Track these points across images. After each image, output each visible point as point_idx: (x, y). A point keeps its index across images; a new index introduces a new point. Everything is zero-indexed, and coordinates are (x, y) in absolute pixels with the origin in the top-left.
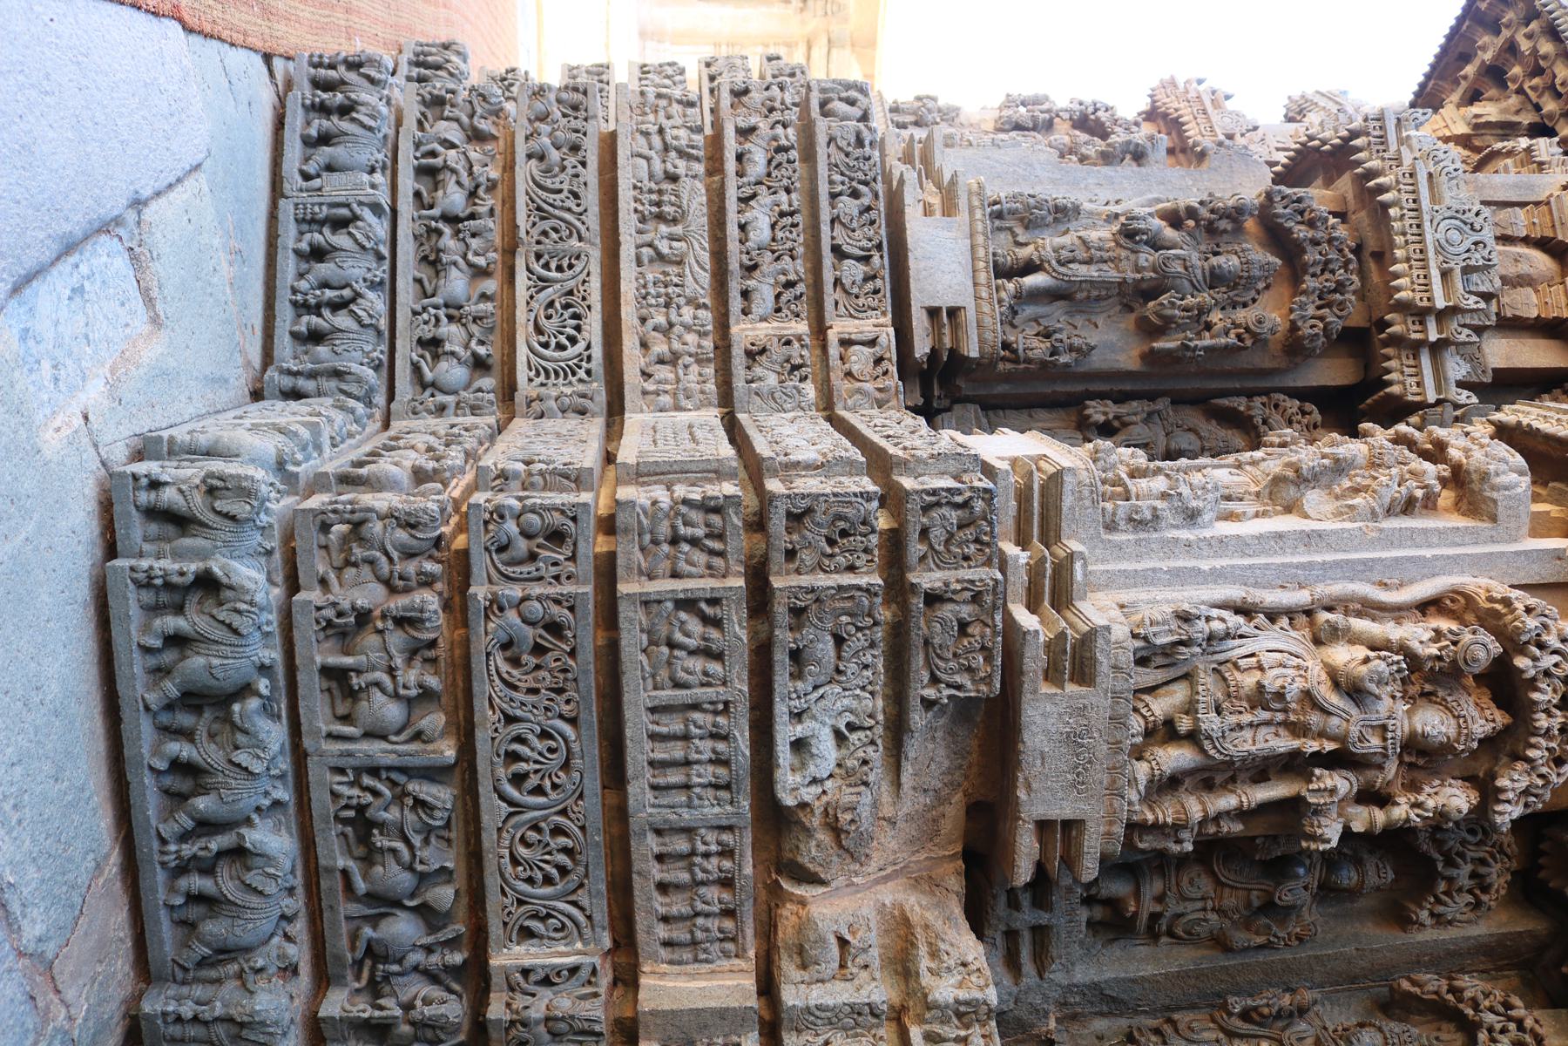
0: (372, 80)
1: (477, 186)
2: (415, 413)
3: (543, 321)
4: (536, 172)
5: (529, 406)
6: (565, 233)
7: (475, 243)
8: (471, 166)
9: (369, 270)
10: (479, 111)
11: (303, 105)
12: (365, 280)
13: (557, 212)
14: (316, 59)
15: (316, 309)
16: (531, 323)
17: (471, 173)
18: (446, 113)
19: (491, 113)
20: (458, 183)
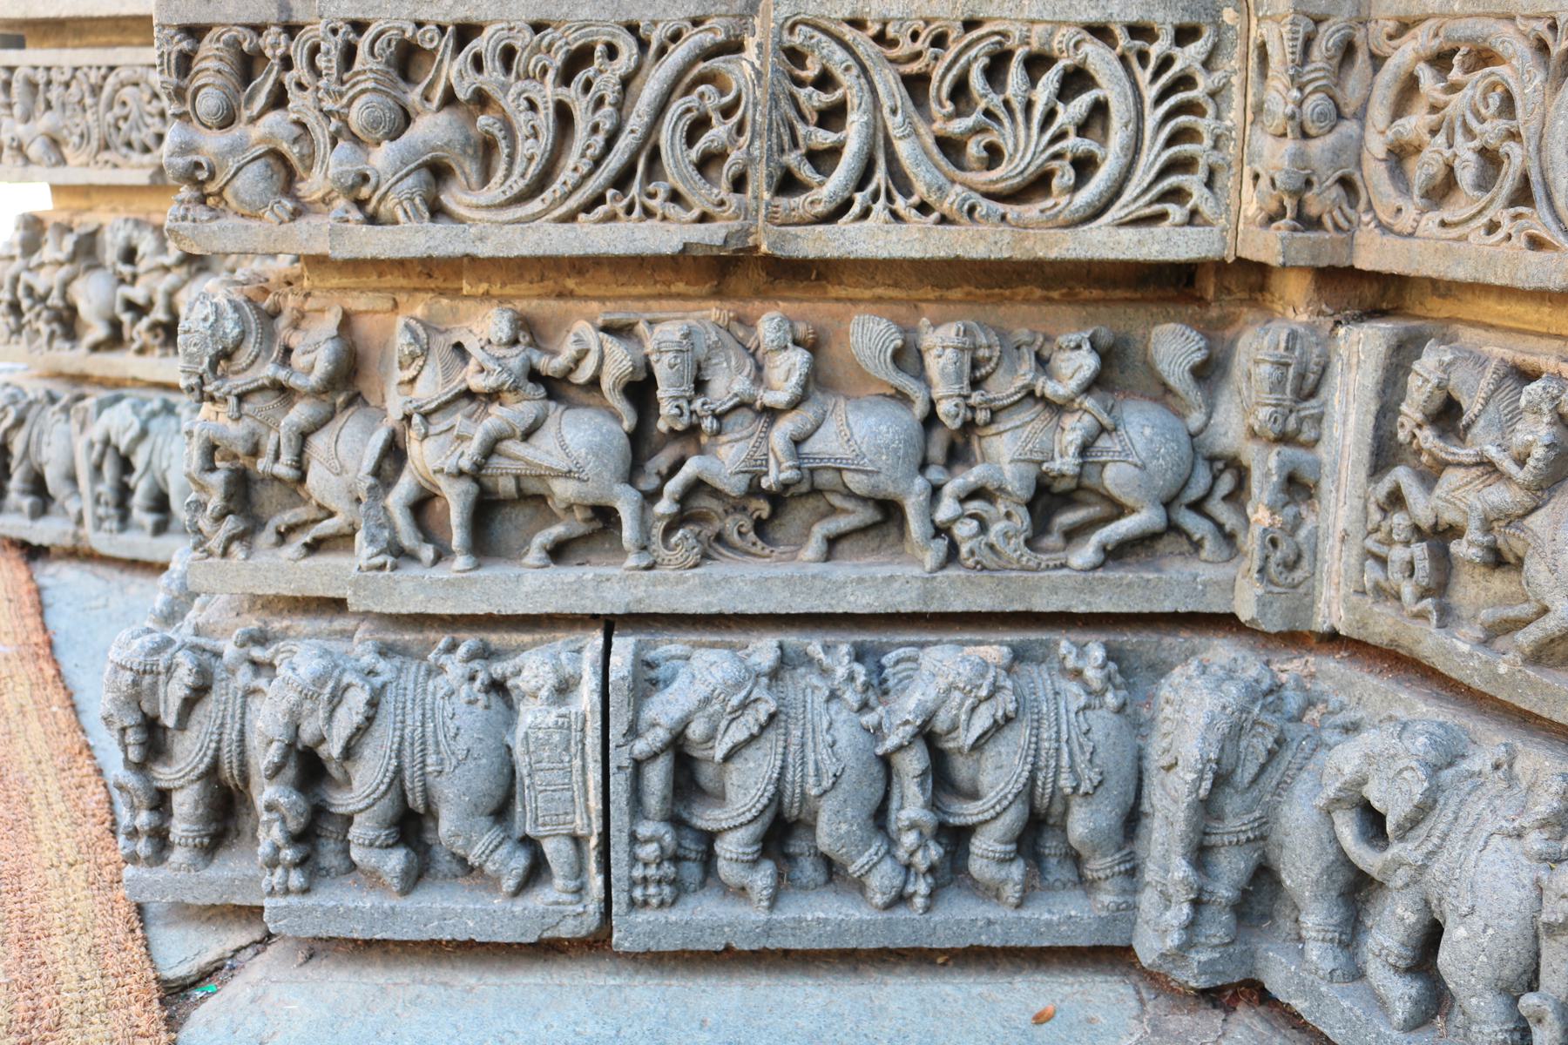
0: (199, 692)
1: (534, 375)
2: (1291, 565)
3: (1007, 174)
4: (495, 191)
5: (1315, 224)
6: (711, 99)
7: (727, 384)
8: (469, 394)
9: (833, 695)
10: (268, 371)
11: (305, 891)
12: (864, 707)
13: (637, 121)
14: (143, 847)
15: (956, 838)
16: (1012, 211)
17: (493, 396)
18: (283, 469)
19: (268, 335)
20: (527, 435)
